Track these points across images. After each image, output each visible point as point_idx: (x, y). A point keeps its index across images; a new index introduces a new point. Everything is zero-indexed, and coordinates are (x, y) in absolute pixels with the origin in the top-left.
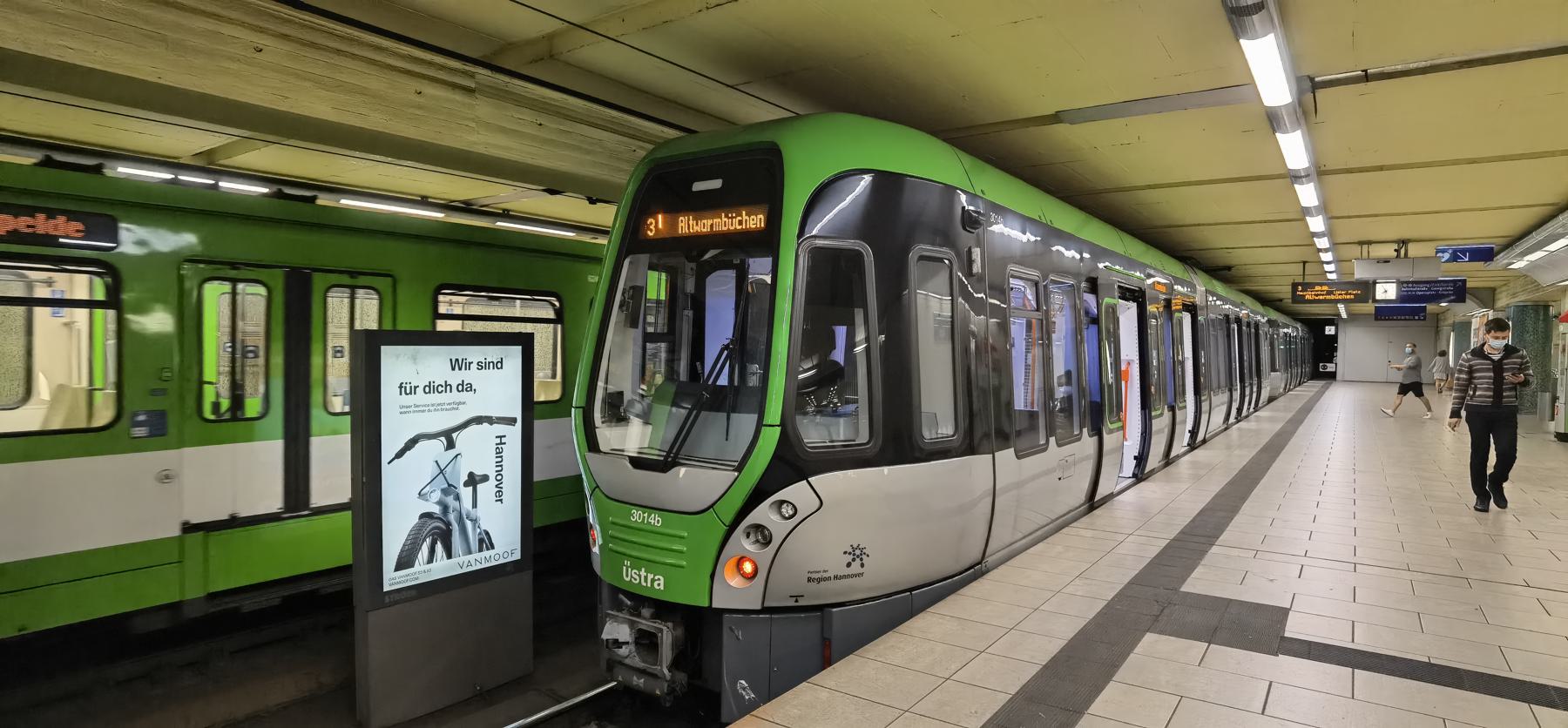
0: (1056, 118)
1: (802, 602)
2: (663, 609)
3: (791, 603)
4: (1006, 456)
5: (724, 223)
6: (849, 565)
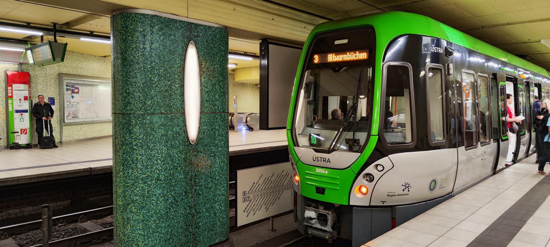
1: (385, 204)
2: (328, 206)
3: (381, 204)
4: (462, 149)
6: (404, 190)
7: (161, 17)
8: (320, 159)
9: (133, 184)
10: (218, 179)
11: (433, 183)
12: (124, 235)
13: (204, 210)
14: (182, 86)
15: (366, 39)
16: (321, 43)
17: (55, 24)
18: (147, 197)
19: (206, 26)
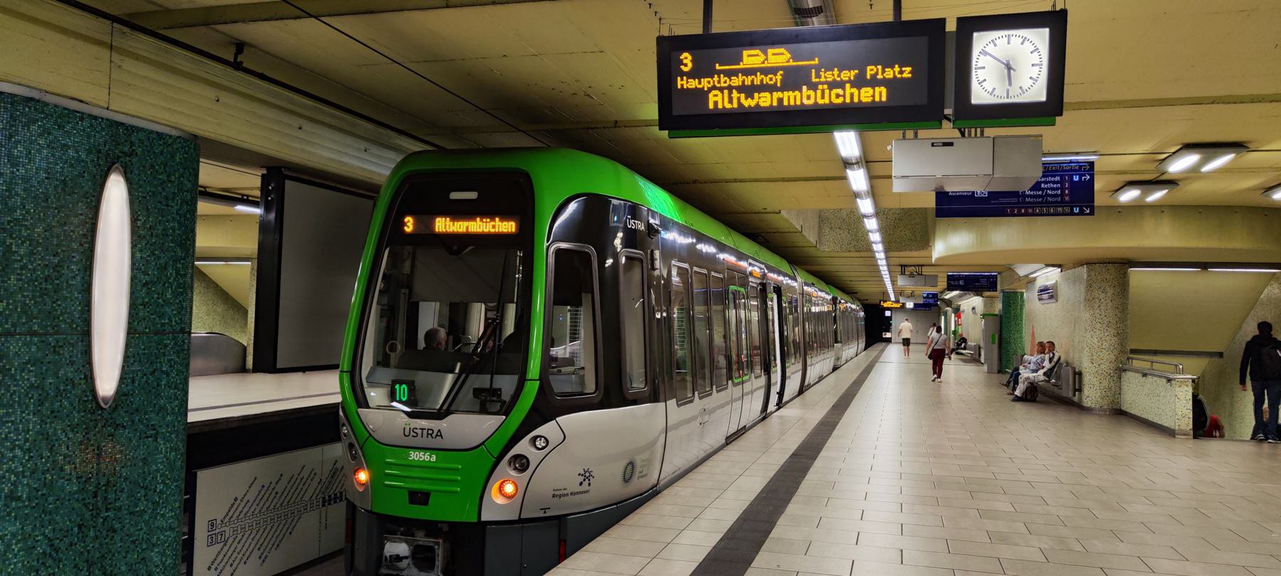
0: (735, 181)
2: (431, 527)
3: (541, 514)
5: (478, 226)
7: (47, 104)
8: (419, 432)
10: (161, 492)
11: (630, 467)
13: (123, 568)
15: (515, 196)
16: (421, 192)
19: (151, 132)
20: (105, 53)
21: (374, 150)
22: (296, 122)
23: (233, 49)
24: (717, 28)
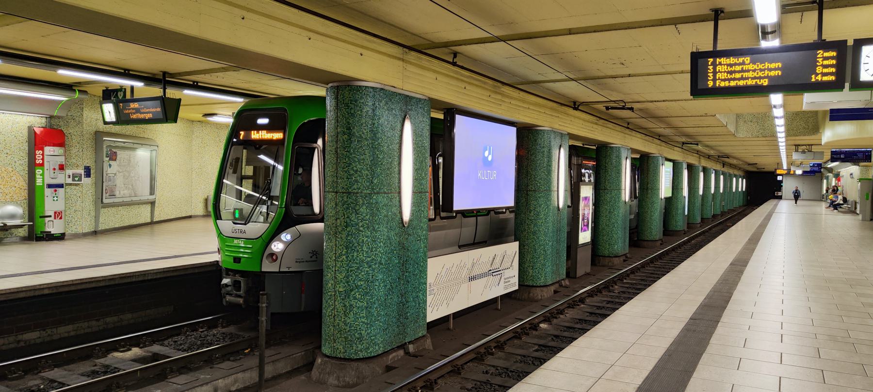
9: (358, 268)
12: (346, 324)
14: (400, 164)
17: (165, 74)
18: (372, 282)
20: (401, 63)
21: (493, 96)
22: (463, 85)
23: (452, 56)
24: (720, 47)
